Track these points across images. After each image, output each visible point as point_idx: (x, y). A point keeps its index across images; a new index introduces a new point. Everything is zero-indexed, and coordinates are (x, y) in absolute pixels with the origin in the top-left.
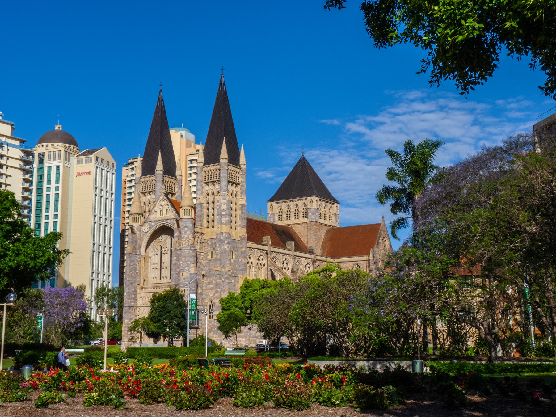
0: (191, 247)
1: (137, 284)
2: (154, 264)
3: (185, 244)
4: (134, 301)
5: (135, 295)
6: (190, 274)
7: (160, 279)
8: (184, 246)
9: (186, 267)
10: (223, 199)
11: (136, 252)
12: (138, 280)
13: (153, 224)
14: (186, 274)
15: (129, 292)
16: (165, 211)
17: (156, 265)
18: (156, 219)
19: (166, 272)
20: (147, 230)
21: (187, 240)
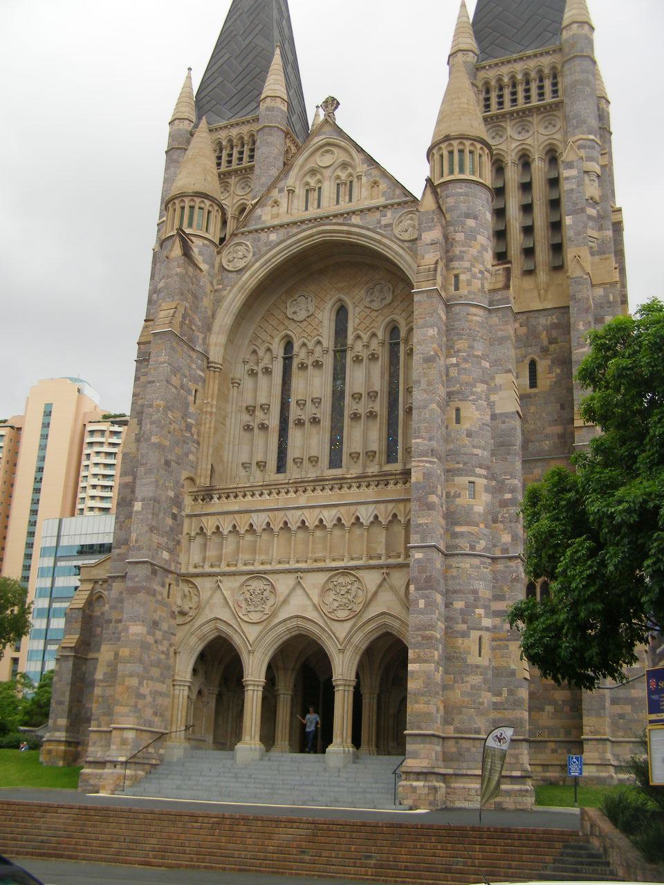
0: (491, 304)
1: (185, 474)
2: (250, 410)
3: (469, 283)
4: (171, 544)
5: (174, 517)
6: (494, 417)
7: (281, 467)
8: (464, 291)
9: (475, 381)
10: (590, 159)
11: (191, 339)
12: (191, 457)
13: (273, 237)
14: (477, 414)
15: (155, 500)
16: (328, 189)
17: (259, 414)
18: (286, 219)
19: (314, 441)
20: (241, 264)
21: (476, 270)
